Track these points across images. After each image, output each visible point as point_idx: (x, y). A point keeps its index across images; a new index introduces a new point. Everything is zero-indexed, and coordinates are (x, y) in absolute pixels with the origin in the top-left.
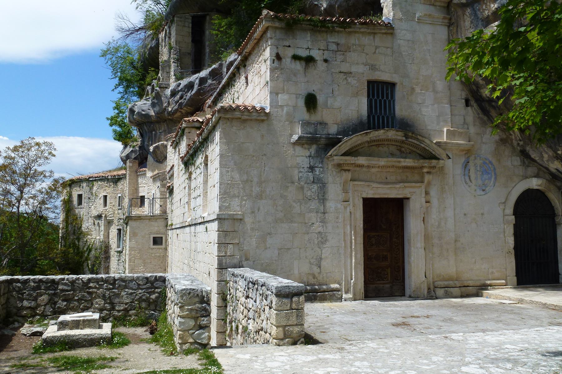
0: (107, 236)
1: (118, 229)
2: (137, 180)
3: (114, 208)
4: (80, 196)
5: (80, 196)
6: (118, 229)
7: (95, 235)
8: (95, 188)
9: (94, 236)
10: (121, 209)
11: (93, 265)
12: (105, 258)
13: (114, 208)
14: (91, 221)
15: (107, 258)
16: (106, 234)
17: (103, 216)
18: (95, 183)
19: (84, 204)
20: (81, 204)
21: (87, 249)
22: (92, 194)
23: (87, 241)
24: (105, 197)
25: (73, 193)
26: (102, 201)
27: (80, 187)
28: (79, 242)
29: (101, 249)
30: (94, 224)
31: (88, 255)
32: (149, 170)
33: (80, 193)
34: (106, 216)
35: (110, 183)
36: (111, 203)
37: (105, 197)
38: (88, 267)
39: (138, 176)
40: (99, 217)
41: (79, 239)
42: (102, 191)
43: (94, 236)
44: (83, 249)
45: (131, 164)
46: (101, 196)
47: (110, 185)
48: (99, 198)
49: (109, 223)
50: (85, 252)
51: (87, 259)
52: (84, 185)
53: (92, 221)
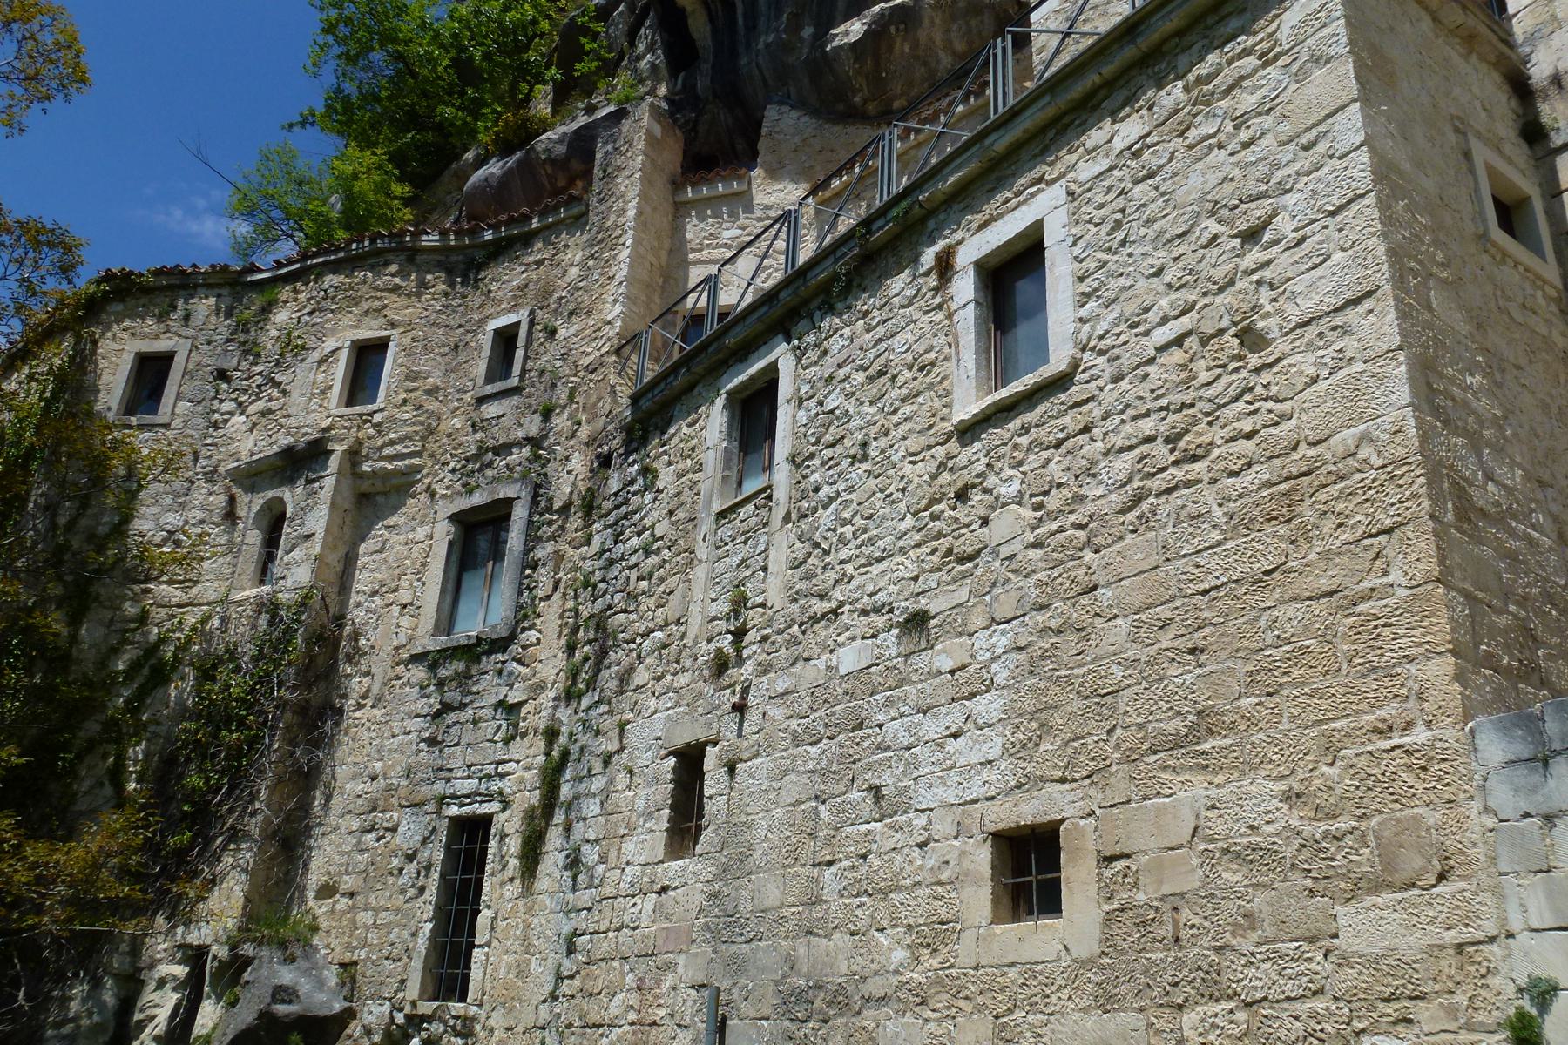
0: (331, 575)
1: (454, 518)
2: (677, 231)
3: (432, 405)
4: (151, 373)
5: (151, 373)
6: (454, 518)
7: (208, 584)
8: (281, 316)
9: (208, 590)
10: (516, 391)
11: (165, 771)
12: (302, 709)
13: (432, 405)
14: (207, 499)
15: (318, 718)
16: (334, 559)
17: (339, 448)
18: (286, 293)
19: (175, 404)
20: (154, 410)
21: (135, 666)
22: (251, 351)
23: (143, 618)
24: (368, 356)
25: (106, 346)
26: (340, 370)
27: (162, 317)
28: (75, 620)
29: (275, 645)
30: (230, 516)
31: (133, 707)
32: (774, 174)
33: (162, 345)
34: (354, 455)
35: (422, 269)
36: (411, 376)
37: (368, 356)
38: (119, 786)
39: (680, 210)
40: (300, 461)
41: (79, 603)
42: (347, 319)
43: (208, 590)
44: (103, 664)
45: (657, 130)
46: (331, 344)
47: (423, 285)
48: (316, 355)
49: (372, 498)
50: (109, 684)
51: (116, 734)
52: (204, 306)
53: (220, 500)
